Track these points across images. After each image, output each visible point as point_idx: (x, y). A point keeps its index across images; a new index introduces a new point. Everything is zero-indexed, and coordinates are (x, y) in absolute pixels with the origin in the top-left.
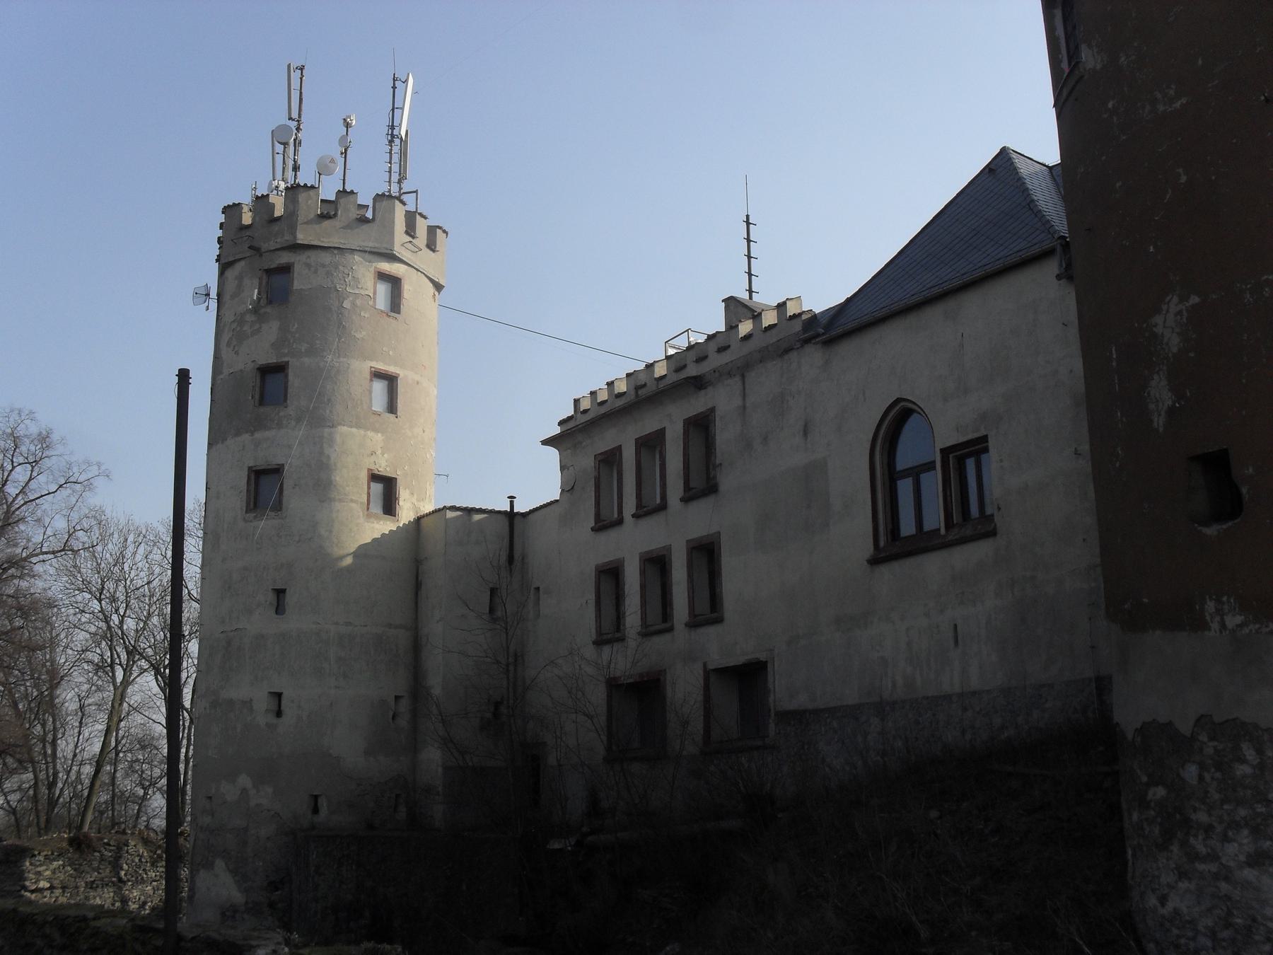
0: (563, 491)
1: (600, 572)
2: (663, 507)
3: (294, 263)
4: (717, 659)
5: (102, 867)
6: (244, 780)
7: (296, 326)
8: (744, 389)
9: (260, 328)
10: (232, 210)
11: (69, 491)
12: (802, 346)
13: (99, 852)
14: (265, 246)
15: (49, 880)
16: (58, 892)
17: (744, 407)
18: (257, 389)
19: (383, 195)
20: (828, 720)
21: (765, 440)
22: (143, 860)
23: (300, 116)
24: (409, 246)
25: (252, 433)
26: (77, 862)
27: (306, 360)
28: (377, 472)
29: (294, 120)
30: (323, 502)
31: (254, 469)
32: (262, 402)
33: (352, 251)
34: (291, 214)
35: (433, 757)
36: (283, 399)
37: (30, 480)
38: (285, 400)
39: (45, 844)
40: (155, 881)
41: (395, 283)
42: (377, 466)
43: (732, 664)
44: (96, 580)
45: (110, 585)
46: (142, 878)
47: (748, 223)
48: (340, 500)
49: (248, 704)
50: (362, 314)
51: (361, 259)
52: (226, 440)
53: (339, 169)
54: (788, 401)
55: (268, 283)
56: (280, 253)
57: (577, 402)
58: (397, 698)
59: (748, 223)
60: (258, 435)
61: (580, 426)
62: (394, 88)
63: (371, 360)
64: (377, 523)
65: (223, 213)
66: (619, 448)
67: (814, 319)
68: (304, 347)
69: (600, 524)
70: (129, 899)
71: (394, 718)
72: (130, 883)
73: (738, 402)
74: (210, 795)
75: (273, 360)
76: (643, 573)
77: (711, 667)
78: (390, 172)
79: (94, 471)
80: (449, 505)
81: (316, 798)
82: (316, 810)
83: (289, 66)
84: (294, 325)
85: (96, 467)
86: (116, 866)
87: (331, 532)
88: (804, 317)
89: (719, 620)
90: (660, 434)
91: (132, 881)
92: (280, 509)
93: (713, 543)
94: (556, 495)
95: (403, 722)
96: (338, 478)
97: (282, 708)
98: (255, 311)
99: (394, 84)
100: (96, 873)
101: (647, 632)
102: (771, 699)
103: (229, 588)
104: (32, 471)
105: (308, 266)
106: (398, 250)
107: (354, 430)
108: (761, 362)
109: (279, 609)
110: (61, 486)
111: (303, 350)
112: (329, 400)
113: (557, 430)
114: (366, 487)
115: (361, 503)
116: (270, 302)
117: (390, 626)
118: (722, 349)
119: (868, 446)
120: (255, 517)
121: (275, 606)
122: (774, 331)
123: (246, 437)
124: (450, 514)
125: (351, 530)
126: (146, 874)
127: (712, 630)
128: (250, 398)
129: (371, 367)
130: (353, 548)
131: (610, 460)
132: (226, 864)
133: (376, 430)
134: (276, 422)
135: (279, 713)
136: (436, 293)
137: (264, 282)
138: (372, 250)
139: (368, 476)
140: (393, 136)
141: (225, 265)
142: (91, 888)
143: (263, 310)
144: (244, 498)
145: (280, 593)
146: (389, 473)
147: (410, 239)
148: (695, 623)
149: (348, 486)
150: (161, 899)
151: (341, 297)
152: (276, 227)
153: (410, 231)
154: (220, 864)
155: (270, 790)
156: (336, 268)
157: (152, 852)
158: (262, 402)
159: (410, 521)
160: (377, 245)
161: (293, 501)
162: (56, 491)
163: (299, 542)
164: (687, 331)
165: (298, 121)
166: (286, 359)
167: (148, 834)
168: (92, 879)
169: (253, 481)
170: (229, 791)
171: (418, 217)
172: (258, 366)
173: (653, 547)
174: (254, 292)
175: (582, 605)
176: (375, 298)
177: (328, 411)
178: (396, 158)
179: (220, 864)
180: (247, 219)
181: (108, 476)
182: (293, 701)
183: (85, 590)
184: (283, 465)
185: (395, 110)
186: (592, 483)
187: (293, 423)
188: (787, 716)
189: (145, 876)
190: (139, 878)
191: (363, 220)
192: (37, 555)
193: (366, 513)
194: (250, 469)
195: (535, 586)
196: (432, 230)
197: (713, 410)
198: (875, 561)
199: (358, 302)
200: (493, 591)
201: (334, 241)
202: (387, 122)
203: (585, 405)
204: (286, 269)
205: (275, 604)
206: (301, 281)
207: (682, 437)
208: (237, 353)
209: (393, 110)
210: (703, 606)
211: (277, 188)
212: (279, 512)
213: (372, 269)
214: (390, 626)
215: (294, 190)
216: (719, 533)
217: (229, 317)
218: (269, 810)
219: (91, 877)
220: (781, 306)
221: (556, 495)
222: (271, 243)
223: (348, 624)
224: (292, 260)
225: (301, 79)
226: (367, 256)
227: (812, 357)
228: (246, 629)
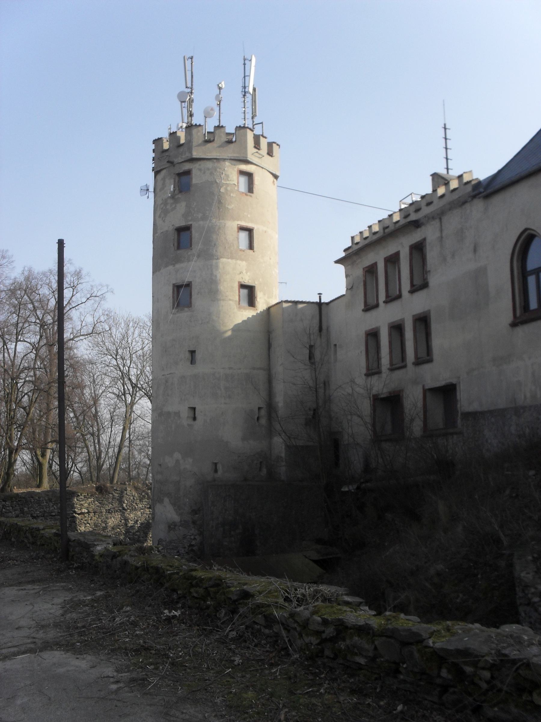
0: (347, 289)
2: (399, 297)
3: (192, 169)
4: (431, 384)
5: (113, 502)
6: (177, 455)
7: (195, 204)
8: (441, 226)
9: (176, 206)
10: (158, 142)
11: (92, 301)
12: (472, 199)
13: (112, 494)
14: (176, 161)
15: (87, 508)
16: (92, 514)
17: (442, 237)
18: (176, 240)
19: (240, 127)
21: (453, 256)
22: (135, 498)
23: (192, 85)
24: (256, 154)
25: (174, 265)
26: (100, 499)
27: (201, 223)
28: (243, 283)
29: (188, 88)
30: (214, 301)
31: (176, 285)
32: (179, 248)
33: (224, 160)
34: (189, 141)
35: (278, 442)
36: (190, 245)
37: (72, 296)
38: (191, 246)
39: (84, 490)
40: (142, 509)
41: (250, 176)
42: (244, 280)
44: (113, 348)
45: (120, 351)
46: (135, 508)
47: (445, 128)
48: (223, 300)
49: (177, 414)
50: (232, 195)
51: (229, 164)
52: (161, 270)
53: (216, 114)
55: (179, 181)
56: (184, 164)
57: (353, 238)
58: (259, 409)
59: (445, 128)
60: (178, 266)
62: (245, 64)
63: (238, 220)
64: (245, 311)
65: (153, 143)
66: (376, 264)
67: (479, 184)
68: (200, 215)
69: (367, 307)
70: (129, 519)
71: (258, 419)
72: (129, 510)
73: (438, 234)
74: (160, 464)
75: (183, 224)
76: (390, 335)
77: (427, 387)
78: (244, 113)
79: (105, 290)
80: (284, 299)
81: (216, 464)
82: (216, 471)
83: (184, 57)
84: (194, 204)
85: (105, 288)
86: (121, 502)
87: (219, 317)
88: (473, 183)
89: (430, 361)
90: (397, 254)
91: (130, 509)
92: (191, 306)
94: (342, 291)
95: (263, 421)
96: (221, 288)
97: (196, 416)
98: (173, 197)
99: (244, 62)
100: (111, 505)
101: (392, 369)
102: (459, 406)
103: (166, 351)
104: (73, 292)
105: (200, 170)
106: (250, 158)
107: (230, 260)
109: (193, 361)
110: (88, 299)
111: (199, 217)
112: (215, 245)
113: (343, 254)
114: (237, 292)
115: (236, 301)
116: (181, 191)
117: (254, 369)
118: (429, 204)
119: (509, 257)
120: (177, 312)
121: (190, 360)
122: (457, 192)
123: (171, 267)
124: (285, 305)
125: (230, 316)
126: (137, 506)
127: (426, 367)
128: (172, 246)
129: (238, 225)
130: (231, 326)
131: (371, 270)
132: (170, 501)
133: (242, 260)
134: (187, 258)
135: (195, 419)
136: (275, 180)
137: (177, 181)
138: (236, 158)
139: (239, 286)
140: (245, 92)
141: (157, 172)
142: (109, 512)
143: (177, 197)
144: (171, 301)
145: (193, 353)
146: (250, 283)
147: (257, 150)
148: (418, 362)
149: (227, 292)
150: (145, 519)
151: (219, 186)
152: (181, 149)
153: (257, 145)
154: (166, 500)
155: (190, 460)
156: (216, 170)
157: (139, 494)
158: (179, 248)
159: (264, 310)
160: (237, 155)
161: (198, 301)
162: (86, 302)
163: (202, 323)
164: (411, 194)
165: (191, 88)
166: (190, 223)
167: (137, 484)
168: (109, 508)
169: (176, 293)
170: (170, 461)
171: (261, 138)
172: (175, 228)
174: (171, 187)
175: (358, 354)
176: (238, 185)
177: (214, 250)
178: (249, 105)
179: (166, 500)
180: (166, 146)
181: (112, 292)
182: (201, 412)
183: (108, 354)
184: (191, 282)
185: (246, 77)
186: (362, 284)
187: (195, 258)
188: (467, 415)
189: (136, 506)
190: (134, 507)
191: (230, 142)
192: (78, 337)
193: (238, 306)
194: (174, 285)
195: (335, 343)
196: (270, 145)
197: (425, 239)
198: (514, 325)
199: (229, 188)
200: (311, 347)
201: (214, 155)
202: (241, 84)
203: (357, 239)
204: (188, 173)
205: (190, 358)
206: (197, 179)
208: (164, 221)
209: (245, 77)
210: (423, 353)
211: (181, 127)
212: (190, 308)
213: (236, 169)
214: (254, 369)
215: (190, 127)
217: (160, 201)
218: (191, 471)
219: (108, 507)
220: (460, 177)
221: (344, 292)
222: (179, 158)
223: (230, 368)
224: (191, 167)
225: (192, 64)
226: (233, 162)
227: (478, 205)
228: (175, 373)
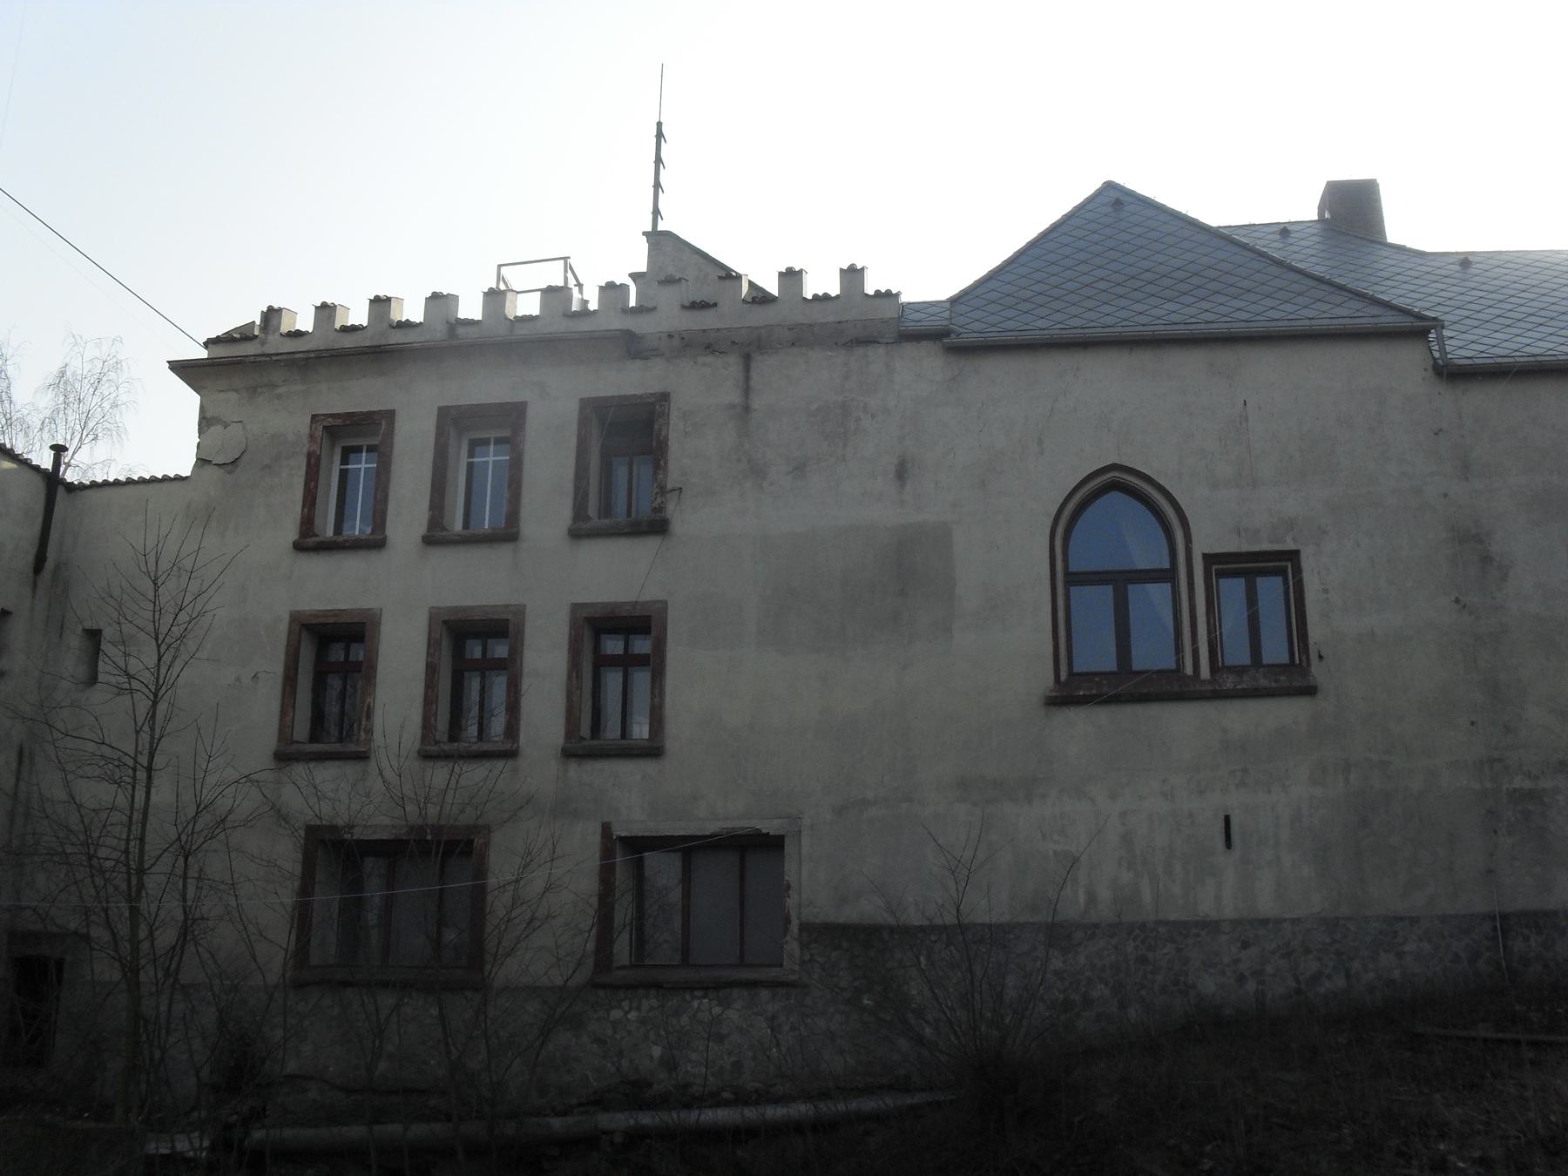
1: (303, 625)
4: (635, 819)
8: (747, 378)
17: (747, 409)
21: (799, 469)
47: (660, 135)
54: (858, 419)
59: (660, 135)
61: (297, 356)
73: (734, 396)
77: (620, 831)
90: (512, 416)
93: (650, 616)
113: (203, 354)
173: (468, 602)
175: (238, 679)
188: (824, 934)
197: (664, 397)
207: (574, 427)
216: (663, 607)
227: (928, 363)
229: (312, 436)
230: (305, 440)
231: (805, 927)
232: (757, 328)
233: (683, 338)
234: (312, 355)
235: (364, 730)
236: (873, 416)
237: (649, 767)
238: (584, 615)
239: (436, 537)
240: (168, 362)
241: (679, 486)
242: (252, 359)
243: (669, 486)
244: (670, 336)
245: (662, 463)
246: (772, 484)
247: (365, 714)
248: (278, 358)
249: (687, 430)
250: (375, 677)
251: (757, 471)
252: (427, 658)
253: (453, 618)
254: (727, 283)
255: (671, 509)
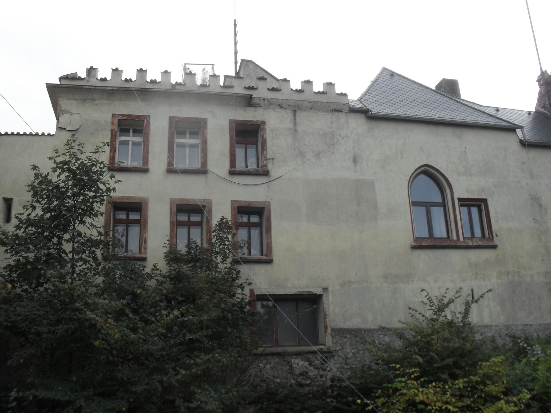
8: (295, 119)
17: (296, 130)
20: (381, 336)
21: (318, 155)
43: (282, 293)
61: (108, 88)
77: (257, 292)
108: (311, 108)
113: (58, 82)
188: (339, 332)
229: (113, 123)
230: (109, 124)
231: (333, 330)
232: (297, 101)
233: (269, 101)
234: (115, 89)
235: (144, 248)
236: (343, 138)
237: (267, 267)
238: (237, 205)
239: (171, 170)
240: (46, 84)
241: (272, 157)
242: (87, 87)
243: (268, 157)
244: (264, 100)
245: (265, 148)
246: (308, 160)
247: (144, 241)
248: (99, 88)
249: (274, 136)
250: (147, 226)
251: (302, 155)
252: (170, 219)
253: (181, 203)
254: (285, 83)
255: (270, 167)
